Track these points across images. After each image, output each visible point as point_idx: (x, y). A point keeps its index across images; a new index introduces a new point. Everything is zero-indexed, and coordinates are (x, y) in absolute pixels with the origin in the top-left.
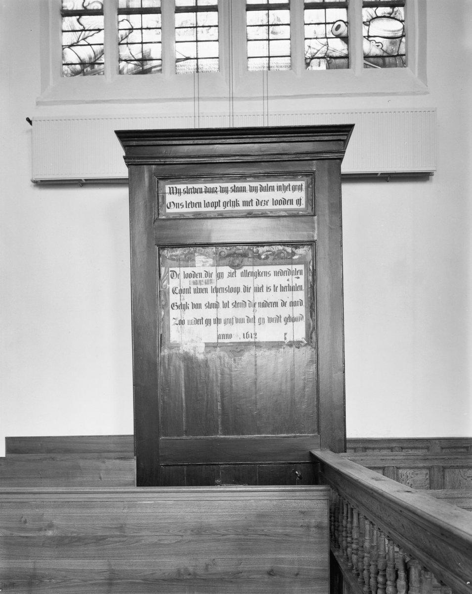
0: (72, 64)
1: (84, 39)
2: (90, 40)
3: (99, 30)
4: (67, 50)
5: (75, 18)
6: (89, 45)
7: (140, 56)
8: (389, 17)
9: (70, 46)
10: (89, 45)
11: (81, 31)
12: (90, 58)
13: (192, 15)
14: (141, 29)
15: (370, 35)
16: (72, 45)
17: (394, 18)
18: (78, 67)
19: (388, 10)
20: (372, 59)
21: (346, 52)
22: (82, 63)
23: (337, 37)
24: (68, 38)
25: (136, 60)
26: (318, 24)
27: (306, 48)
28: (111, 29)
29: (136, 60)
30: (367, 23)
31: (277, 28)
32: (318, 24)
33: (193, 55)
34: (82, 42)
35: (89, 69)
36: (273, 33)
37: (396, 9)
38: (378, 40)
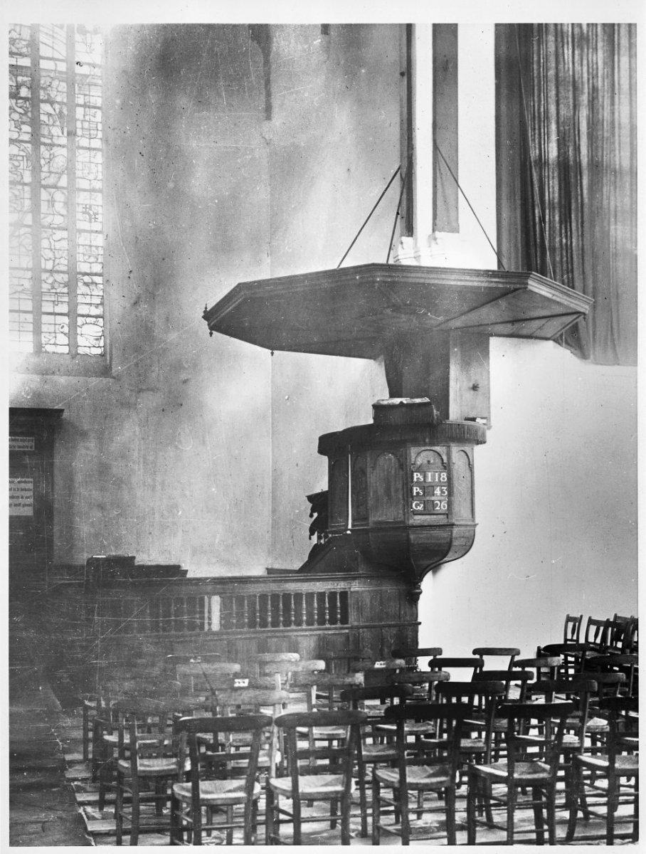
19: (94, 319)
38: (86, 336)
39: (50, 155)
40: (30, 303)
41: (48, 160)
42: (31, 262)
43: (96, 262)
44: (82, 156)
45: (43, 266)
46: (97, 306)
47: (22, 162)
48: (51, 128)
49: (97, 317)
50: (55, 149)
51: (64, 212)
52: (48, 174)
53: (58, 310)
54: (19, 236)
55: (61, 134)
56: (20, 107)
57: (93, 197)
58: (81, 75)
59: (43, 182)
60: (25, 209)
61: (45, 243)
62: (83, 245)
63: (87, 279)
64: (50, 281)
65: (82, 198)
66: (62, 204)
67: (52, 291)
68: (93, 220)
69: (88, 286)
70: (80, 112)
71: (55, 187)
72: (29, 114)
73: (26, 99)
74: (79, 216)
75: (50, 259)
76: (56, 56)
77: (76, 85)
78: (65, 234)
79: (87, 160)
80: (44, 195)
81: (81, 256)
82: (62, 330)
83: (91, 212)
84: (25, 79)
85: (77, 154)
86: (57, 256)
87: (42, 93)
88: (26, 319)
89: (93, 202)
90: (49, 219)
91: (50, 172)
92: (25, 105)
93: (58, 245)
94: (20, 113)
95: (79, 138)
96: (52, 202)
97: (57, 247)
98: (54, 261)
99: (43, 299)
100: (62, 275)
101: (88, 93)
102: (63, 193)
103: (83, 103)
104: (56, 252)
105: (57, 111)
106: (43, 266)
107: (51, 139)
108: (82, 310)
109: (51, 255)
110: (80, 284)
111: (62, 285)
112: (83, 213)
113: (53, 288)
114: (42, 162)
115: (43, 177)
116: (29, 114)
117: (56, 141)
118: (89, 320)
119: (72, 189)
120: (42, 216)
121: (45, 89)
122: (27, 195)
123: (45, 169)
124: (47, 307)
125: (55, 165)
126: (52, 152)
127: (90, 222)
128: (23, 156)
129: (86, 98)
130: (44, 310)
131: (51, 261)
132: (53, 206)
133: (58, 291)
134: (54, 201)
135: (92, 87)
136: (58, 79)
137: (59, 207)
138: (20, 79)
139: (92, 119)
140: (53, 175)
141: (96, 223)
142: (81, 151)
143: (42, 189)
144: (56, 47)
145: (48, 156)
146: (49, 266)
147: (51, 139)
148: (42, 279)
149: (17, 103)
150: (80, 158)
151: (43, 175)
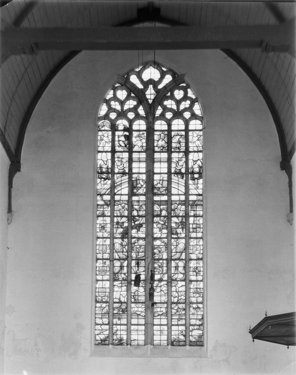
0: (98, 340)
1: (102, 333)
2: (104, 333)
3: (107, 330)
4: (97, 336)
5: (99, 326)
6: (104, 334)
7: (119, 339)
8: (198, 329)
9: (97, 335)
10: (104, 334)
11: (101, 330)
12: (104, 339)
13: (137, 326)
14: (120, 330)
15: (192, 334)
16: (98, 334)
17: (200, 330)
18: (100, 341)
19: (198, 327)
20: (193, 342)
21: (184, 340)
22: (101, 340)
23: (182, 335)
24: (97, 332)
25: (118, 340)
26: (176, 331)
27: (172, 338)
28: (111, 329)
29: (118, 340)
30: (192, 331)
31: (163, 332)
32: (176, 331)
33: (137, 339)
34: (102, 334)
35: (103, 342)
36: (162, 333)
37: (200, 327)
38: (195, 336)
39: (177, 243)
40: (166, 320)
41: (175, 246)
42: (167, 299)
43: (200, 297)
44: (193, 242)
45: (173, 301)
46: (200, 320)
47: (162, 249)
48: (177, 230)
49: (200, 325)
50: (179, 240)
51: (183, 272)
52: (175, 253)
53: (180, 323)
54: (161, 286)
55: (182, 232)
56: (162, 221)
57: (198, 263)
58: (192, 201)
59: (173, 258)
60: (164, 272)
61: (174, 289)
62: (193, 288)
63: (195, 306)
64: (176, 308)
65: (193, 264)
66: (182, 268)
67: (177, 313)
68: (198, 275)
69: (195, 309)
70: (191, 220)
71: (179, 259)
72: (166, 224)
73: (165, 216)
74: (191, 273)
75: (176, 297)
76: (180, 193)
77: (190, 206)
78: (184, 283)
79: (195, 244)
80: (173, 264)
81: (192, 294)
82: (182, 334)
83: (197, 271)
84: (165, 206)
85: (190, 241)
86: (180, 295)
87: (173, 212)
88: (164, 329)
89: (198, 265)
90: (176, 276)
91: (176, 252)
92: (164, 220)
93: (180, 289)
94: (162, 224)
95: (191, 233)
96: (177, 268)
97: (180, 290)
98: (178, 297)
99: (173, 318)
100: (182, 305)
101: (195, 209)
102: (183, 262)
103: (193, 215)
104: (179, 293)
105: (180, 221)
106: (173, 301)
107: (177, 235)
108: (193, 322)
109: (177, 295)
110: (191, 309)
111: (182, 310)
112: (193, 271)
113: (177, 312)
114: (173, 247)
115: (173, 255)
116: (166, 224)
117: (179, 236)
118: (196, 327)
119: (188, 260)
120: (172, 275)
121: (174, 210)
122: (165, 265)
123: (174, 251)
124: (174, 322)
125: (179, 249)
126: (177, 242)
127: (197, 276)
128: (163, 245)
129: (195, 212)
130: (173, 323)
131: (177, 298)
132: (178, 269)
133: (180, 313)
134: (179, 267)
135: (198, 206)
136: (181, 204)
137: (181, 269)
138: (162, 207)
139: (198, 222)
140: (178, 253)
141: (200, 276)
142: (192, 240)
143: (172, 261)
144: (179, 188)
145: (175, 244)
146: (175, 300)
147: (177, 235)
148: (172, 307)
149: (160, 219)
150: (191, 244)
151: (173, 254)
